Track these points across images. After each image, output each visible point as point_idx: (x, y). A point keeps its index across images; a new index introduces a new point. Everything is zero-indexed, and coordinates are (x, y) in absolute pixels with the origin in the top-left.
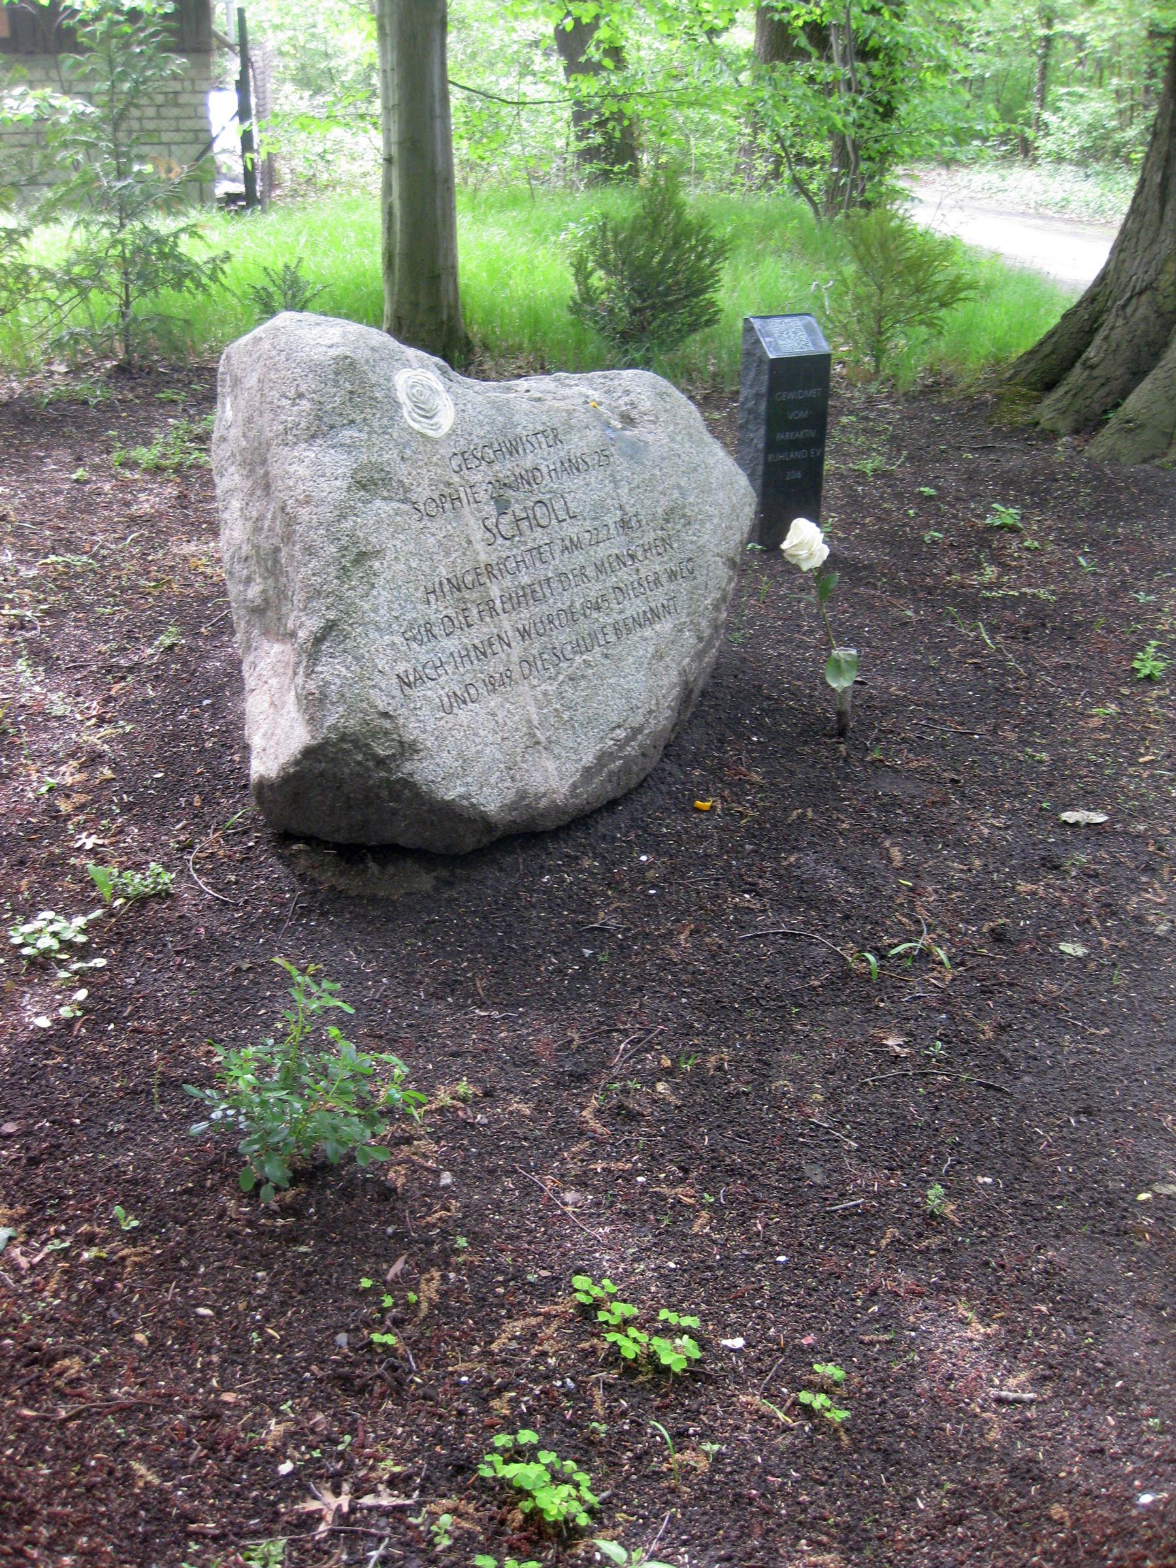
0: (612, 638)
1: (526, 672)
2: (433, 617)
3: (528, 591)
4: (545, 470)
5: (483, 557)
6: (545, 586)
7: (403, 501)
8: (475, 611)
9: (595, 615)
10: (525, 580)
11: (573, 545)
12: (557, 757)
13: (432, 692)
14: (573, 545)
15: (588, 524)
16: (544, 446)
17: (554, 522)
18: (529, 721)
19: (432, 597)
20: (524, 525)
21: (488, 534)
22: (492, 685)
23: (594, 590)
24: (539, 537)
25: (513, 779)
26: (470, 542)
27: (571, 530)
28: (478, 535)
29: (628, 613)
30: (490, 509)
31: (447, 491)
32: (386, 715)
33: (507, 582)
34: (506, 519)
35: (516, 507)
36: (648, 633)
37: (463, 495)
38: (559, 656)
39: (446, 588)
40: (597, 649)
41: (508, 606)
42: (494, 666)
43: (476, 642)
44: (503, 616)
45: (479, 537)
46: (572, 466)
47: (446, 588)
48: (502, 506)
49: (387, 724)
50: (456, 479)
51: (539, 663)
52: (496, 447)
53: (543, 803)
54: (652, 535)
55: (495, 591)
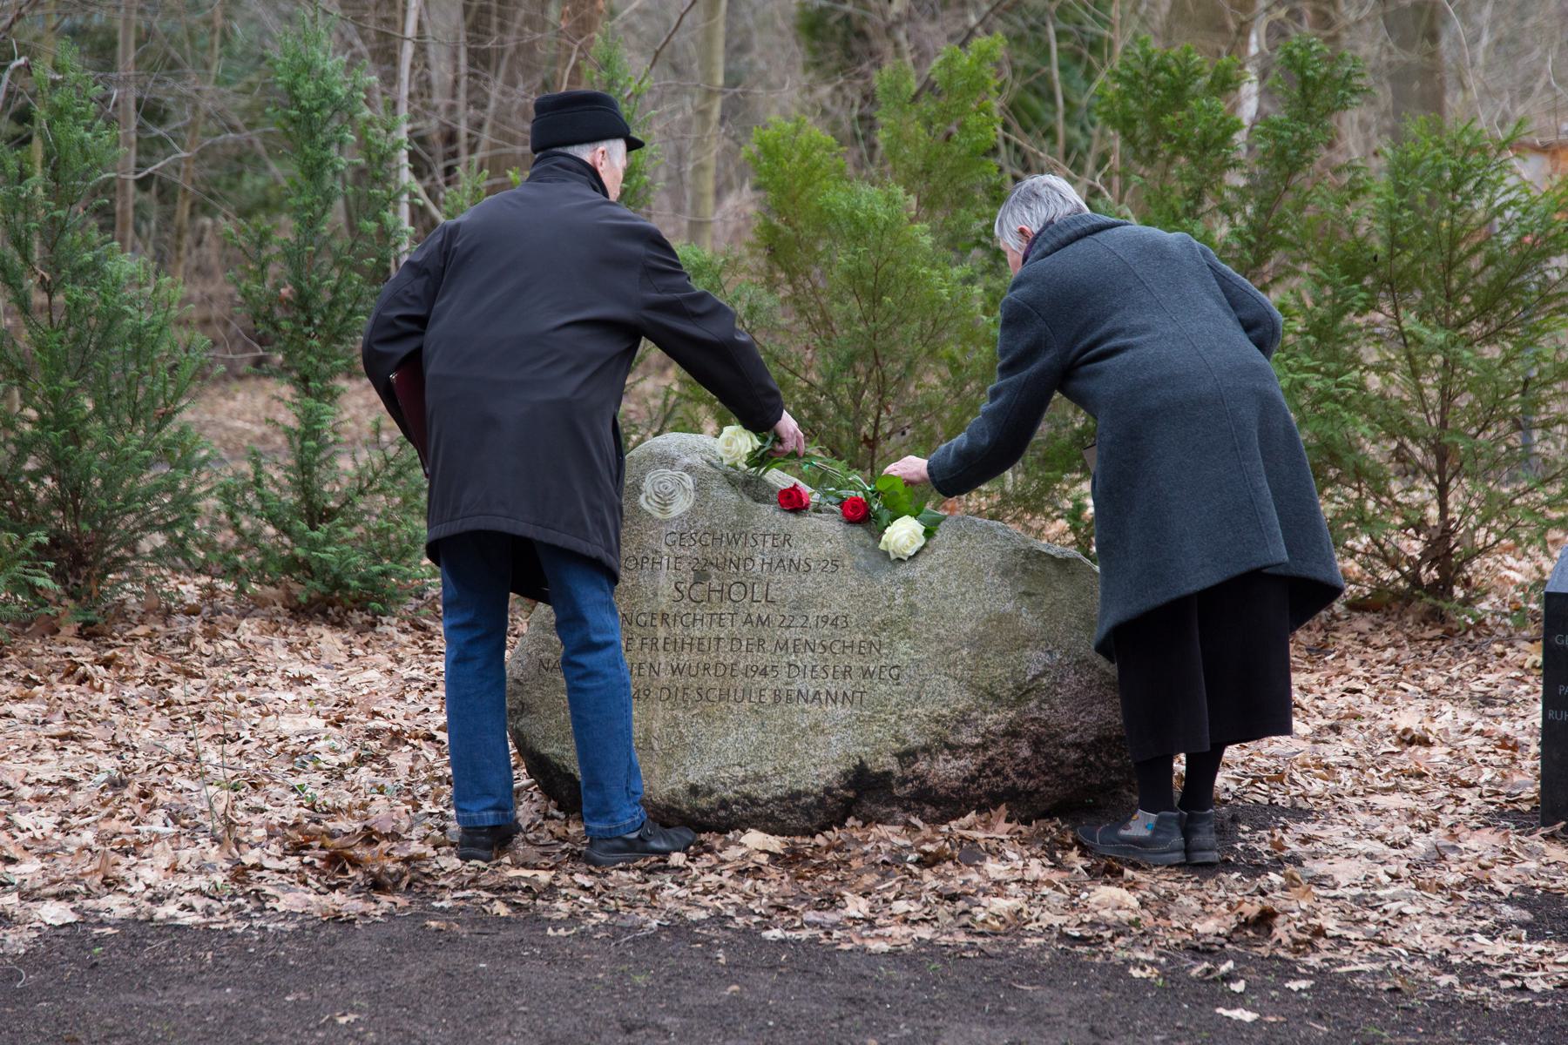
3: (696, 642)
4: (758, 561)
6: (714, 643)
8: (638, 642)
9: (757, 678)
10: (698, 634)
15: (785, 611)
16: (769, 544)
21: (676, 594)
23: (762, 659)
26: (655, 595)
29: (795, 687)
31: (651, 556)
33: (678, 629)
34: (698, 588)
35: (715, 583)
37: (665, 562)
48: (701, 576)
50: (665, 550)
52: (718, 535)
54: (860, 637)
55: (661, 632)
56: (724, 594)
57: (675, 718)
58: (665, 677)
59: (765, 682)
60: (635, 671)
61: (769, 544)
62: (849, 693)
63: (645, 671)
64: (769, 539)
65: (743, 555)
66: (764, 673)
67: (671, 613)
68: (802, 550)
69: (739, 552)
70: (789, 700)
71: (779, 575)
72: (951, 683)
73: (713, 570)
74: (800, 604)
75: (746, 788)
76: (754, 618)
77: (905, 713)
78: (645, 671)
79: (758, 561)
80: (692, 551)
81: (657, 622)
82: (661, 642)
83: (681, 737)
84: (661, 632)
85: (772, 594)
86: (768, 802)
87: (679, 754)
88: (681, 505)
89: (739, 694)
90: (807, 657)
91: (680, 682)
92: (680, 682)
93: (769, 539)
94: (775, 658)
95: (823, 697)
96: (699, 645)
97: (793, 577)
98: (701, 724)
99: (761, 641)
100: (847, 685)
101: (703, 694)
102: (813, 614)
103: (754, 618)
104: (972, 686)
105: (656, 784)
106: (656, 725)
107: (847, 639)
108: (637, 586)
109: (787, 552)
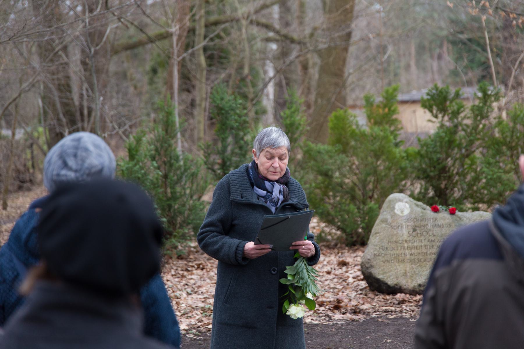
4: (429, 225)
8: (399, 248)
15: (438, 238)
18: (405, 270)
20: (419, 235)
27: (431, 238)
30: (412, 230)
33: (410, 244)
35: (418, 231)
46: (439, 226)
48: (414, 230)
50: (404, 224)
53: (405, 287)
55: (406, 245)
56: (422, 234)
58: (408, 256)
63: (403, 255)
67: (408, 239)
68: (441, 222)
69: (423, 223)
71: (435, 229)
73: (418, 228)
78: (403, 255)
80: (411, 223)
81: (404, 242)
83: (415, 272)
84: (406, 245)
85: (435, 234)
87: (415, 276)
88: (407, 212)
91: (413, 257)
92: (413, 257)
96: (416, 248)
97: (439, 229)
98: (419, 268)
101: (419, 260)
105: (409, 284)
106: (408, 269)
108: (398, 233)
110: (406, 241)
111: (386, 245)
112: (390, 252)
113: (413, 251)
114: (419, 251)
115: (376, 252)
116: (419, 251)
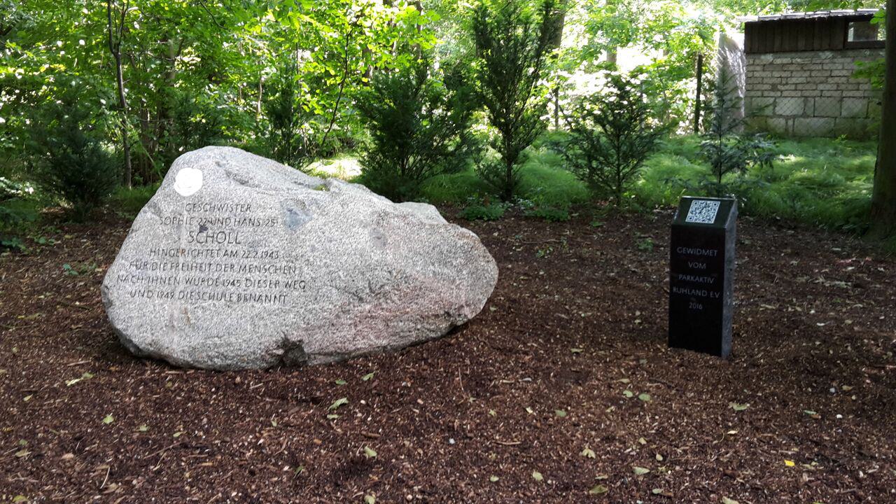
0: (235, 298)
1: (181, 297)
2: (149, 262)
4: (233, 220)
5: (183, 246)
6: (207, 266)
7: (159, 216)
8: (169, 265)
9: (230, 287)
10: (200, 261)
11: (234, 254)
12: (181, 336)
13: (129, 287)
14: (234, 254)
16: (239, 210)
17: (226, 242)
18: (172, 316)
19: (153, 254)
22: (161, 295)
23: (234, 275)
24: (215, 246)
25: (152, 334)
28: (185, 235)
32: (107, 287)
35: (210, 232)
36: (257, 305)
38: (201, 296)
39: (161, 252)
40: (223, 300)
41: (185, 268)
42: (167, 289)
43: (163, 277)
44: (181, 271)
45: (185, 237)
47: (161, 252)
48: (203, 228)
49: (106, 291)
51: (189, 296)
53: (166, 352)
54: (284, 263)
55: (181, 260)
57: (186, 309)
59: (232, 288)
60: (167, 282)
61: (239, 210)
62: (278, 296)
64: (239, 207)
65: (226, 216)
66: (233, 284)
70: (246, 300)
72: (334, 291)
74: (253, 245)
75: (222, 350)
76: (229, 252)
77: (309, 307)
79: (233, 220)
81: (179, 254)
82: (181, 265)
86: (234, 357)
89: (220, 296)
90: (256, 276)
93: (239, 207)
94: (239, 275)
95: (264, 299)
99: (232, 266)
100: (276, 291)
102: (261, 250)
103: (229, 252)
104: (345, 290)
106: (176, 314)
107: (278, 265)
109: (248, 214)
110: (183, 251)
111: (146, 258)
112: (150, 272)
113: (195, 274)
114: (203, 275)
115: (121, 274)
116: (203, 275)
